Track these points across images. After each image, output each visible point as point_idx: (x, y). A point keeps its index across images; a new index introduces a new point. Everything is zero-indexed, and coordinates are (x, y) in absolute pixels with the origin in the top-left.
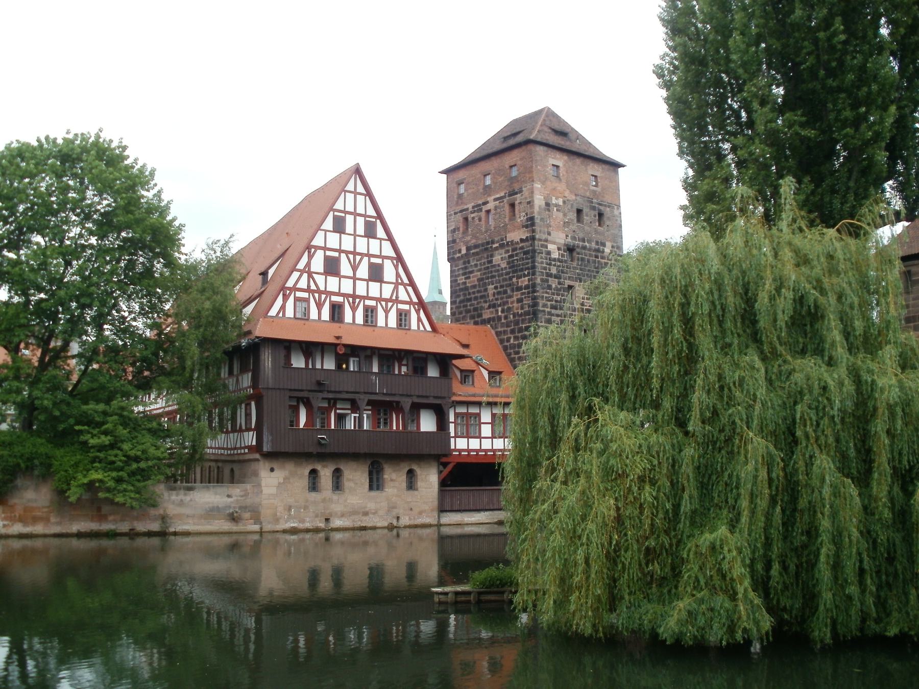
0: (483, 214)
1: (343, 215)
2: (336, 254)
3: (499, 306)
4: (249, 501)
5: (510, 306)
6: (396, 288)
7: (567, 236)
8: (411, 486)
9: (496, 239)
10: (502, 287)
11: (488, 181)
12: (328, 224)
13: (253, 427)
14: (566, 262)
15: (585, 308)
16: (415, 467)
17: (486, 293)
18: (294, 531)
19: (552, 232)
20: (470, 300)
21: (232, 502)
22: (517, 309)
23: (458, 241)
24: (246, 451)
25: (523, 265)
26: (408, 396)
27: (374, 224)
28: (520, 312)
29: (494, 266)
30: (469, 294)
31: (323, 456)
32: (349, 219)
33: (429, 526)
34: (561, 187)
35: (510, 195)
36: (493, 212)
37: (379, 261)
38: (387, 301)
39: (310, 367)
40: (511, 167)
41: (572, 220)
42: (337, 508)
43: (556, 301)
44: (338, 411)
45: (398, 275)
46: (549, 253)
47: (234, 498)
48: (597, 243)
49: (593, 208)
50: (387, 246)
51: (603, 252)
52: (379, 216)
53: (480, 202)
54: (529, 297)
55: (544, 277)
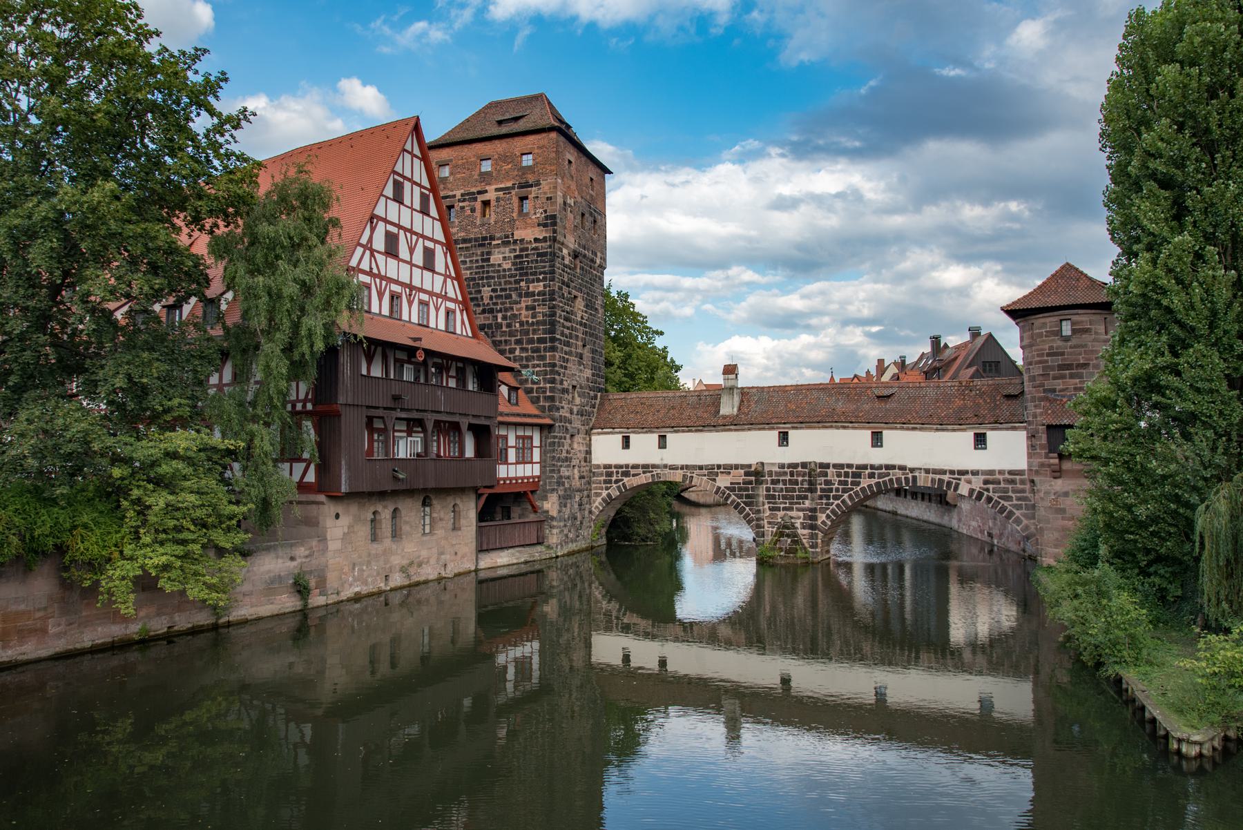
0: (478, 205)
1: (401, 180)
2: (394, 230)
3: (500, 311)
5: (515, 312)
6: (445, 281)
9: (498, 235)
10: (502, 290)
11: (486, 167)
12: (389, 191)
16: (458, 502)
17: (479, 296)
22: (526, 317)
25: (535, 268)
27: (428, 196)
28: (530, 321)
29: (493, 265)
31: (382, 495)
32: (407, 185)
33: (470, 572)
34: (573, 187)
35: (521, 187)
36: (493, 203)
37: (430, 245)
38: (438, 296)
39: (422, 381)
44: (396, 434)
45: (447, 266)
49: (591, 214)
50: (438, 225)
53: (474, 190)
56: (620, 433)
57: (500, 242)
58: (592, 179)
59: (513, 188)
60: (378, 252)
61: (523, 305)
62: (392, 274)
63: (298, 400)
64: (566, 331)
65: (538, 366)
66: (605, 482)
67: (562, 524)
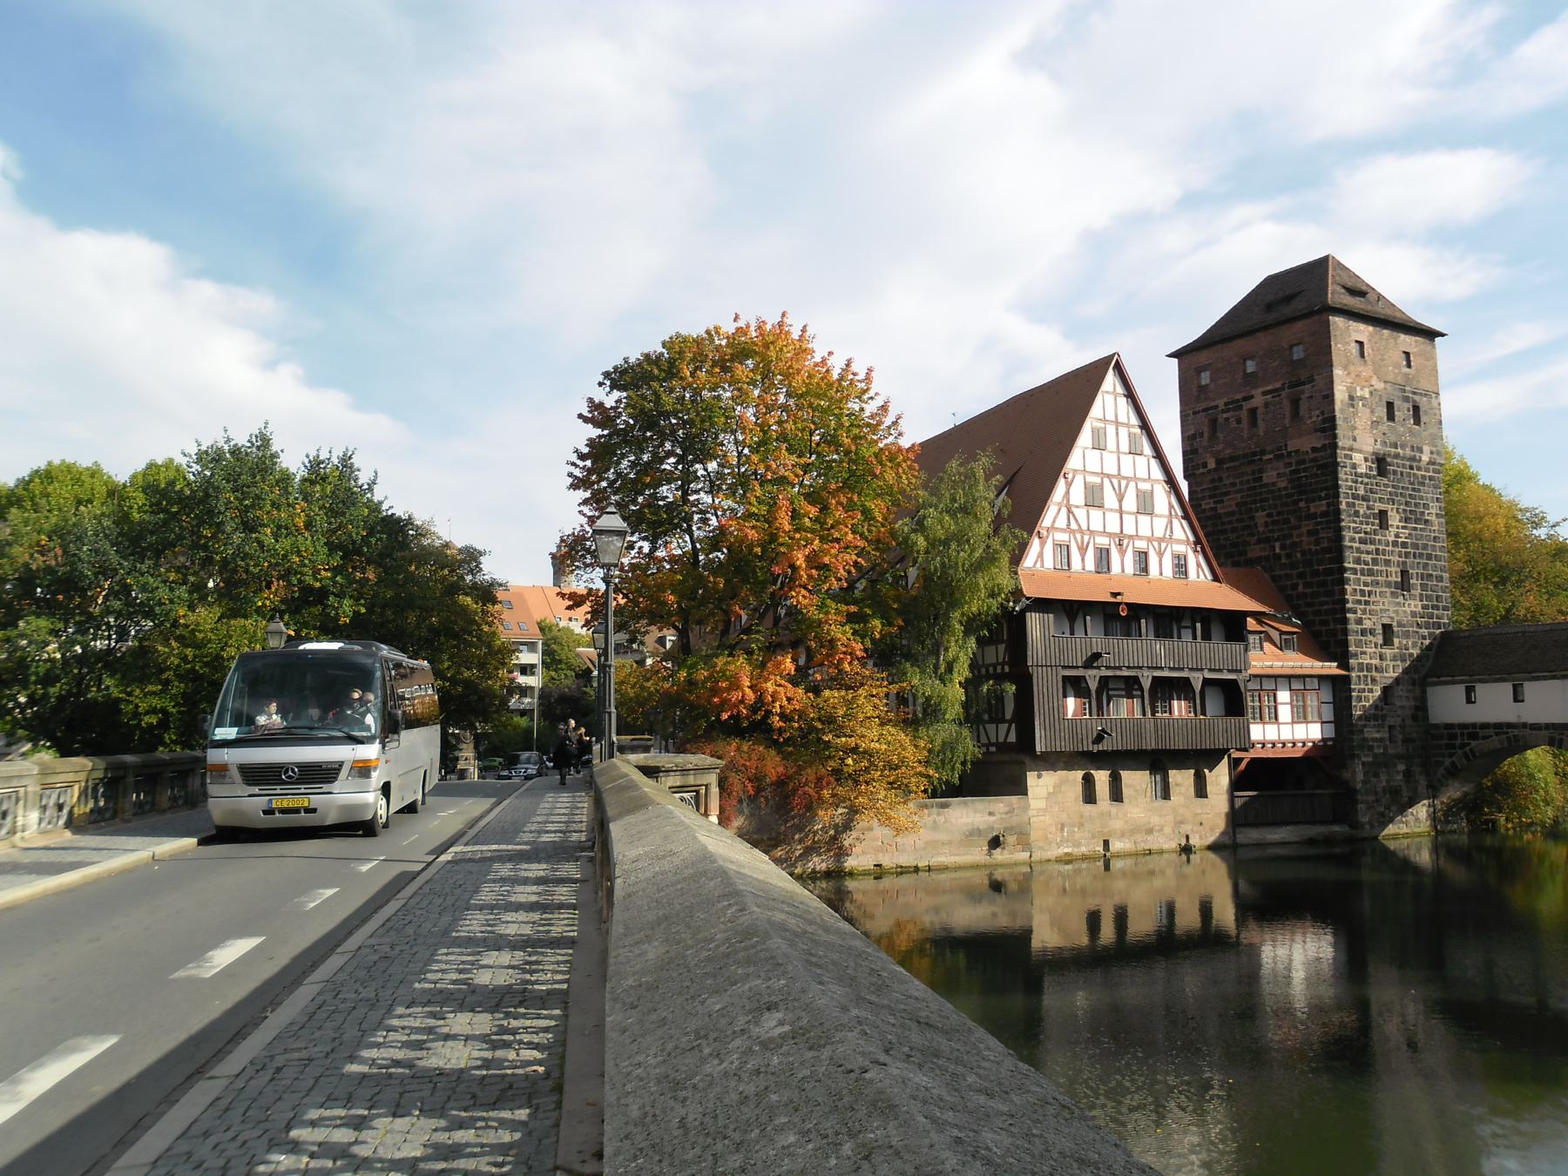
0: (1244, 414)
2: (1097, 480)
3: (1277, 540)
4: (1015, 820)
7: (1376, 441)
8: (1201, 791)
10: (1279, 514)
11: (1251, 366)
13: (1008, 716)
14: (1374, 477)
17: (1252, 523)
18: (1067, 860)
20: (1224, 532)
21: (994, 822)
23: (1200, 451)
24: (993, 749)
26: (1197, 669)
28: (1313, 548)
30: (1223, 524)
32: (1111, 429)
35: (1292, 386)
36: (1259, 412)
37: (1145, 486)
38: (1160, 540)
40: (1291, 347)
41: (1382, 418)
42: (1117, 824)
43: (1366, 533)
45: (1171, 506)
46: (1354, 466)
47: (998, 816)
48: (1412, 447)
49: (1406, 399)
50: (1154, 463)
51: (1420, 460)
52: (1145, 426)
53: (1238, 396)
54: (1330, 528)
55: (1351, 500)
56: (1462, 682)
57: (1271, 456)
58: (1407, 354)
59: (1282, 389)
60: (1077, 507)
61: (1304, 530)
62: (1096, 525)
63: (998, 664)
64: (1369, 558)
65: (1327, 603)
66: (1448, 746)
67: (1371, 798)
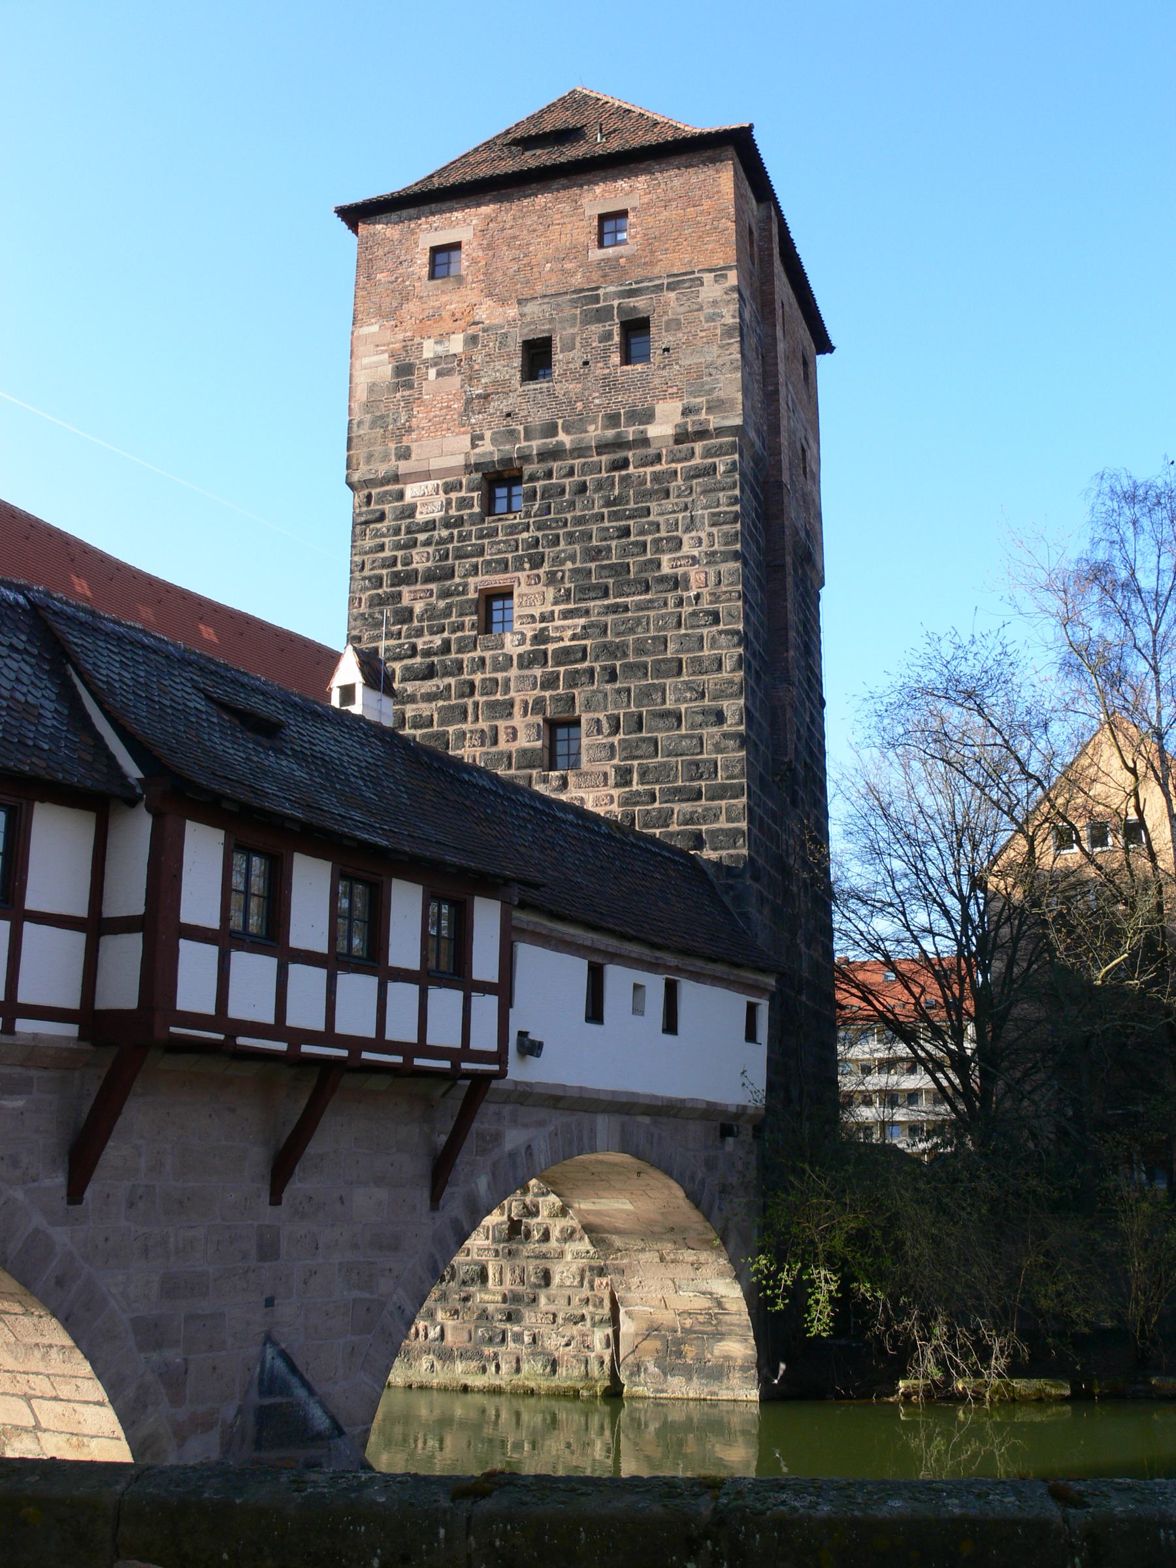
15: (551, 647)
19: (414, 446)
43: (427, 653)
48: (613, 420)
51: (644, 442)
